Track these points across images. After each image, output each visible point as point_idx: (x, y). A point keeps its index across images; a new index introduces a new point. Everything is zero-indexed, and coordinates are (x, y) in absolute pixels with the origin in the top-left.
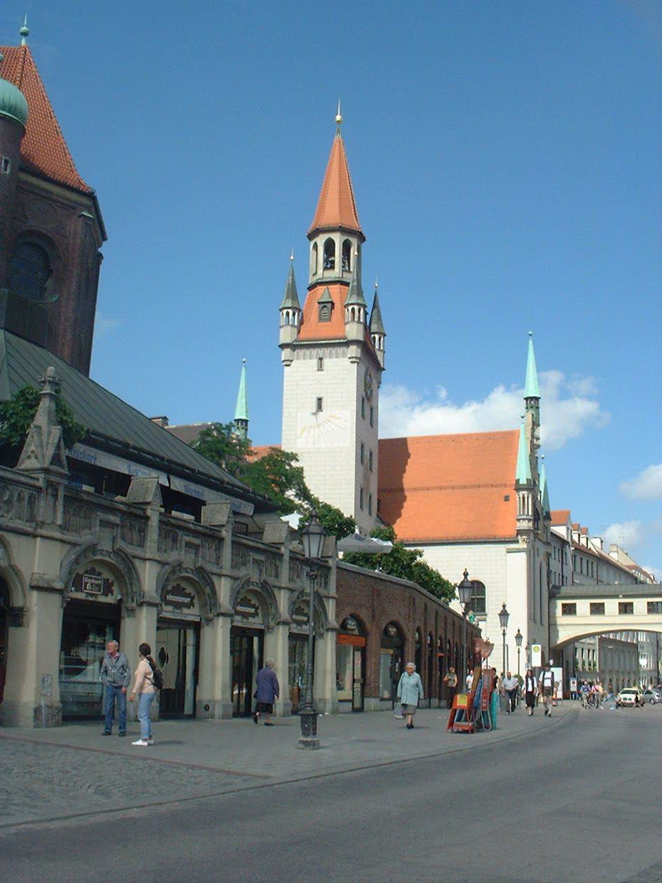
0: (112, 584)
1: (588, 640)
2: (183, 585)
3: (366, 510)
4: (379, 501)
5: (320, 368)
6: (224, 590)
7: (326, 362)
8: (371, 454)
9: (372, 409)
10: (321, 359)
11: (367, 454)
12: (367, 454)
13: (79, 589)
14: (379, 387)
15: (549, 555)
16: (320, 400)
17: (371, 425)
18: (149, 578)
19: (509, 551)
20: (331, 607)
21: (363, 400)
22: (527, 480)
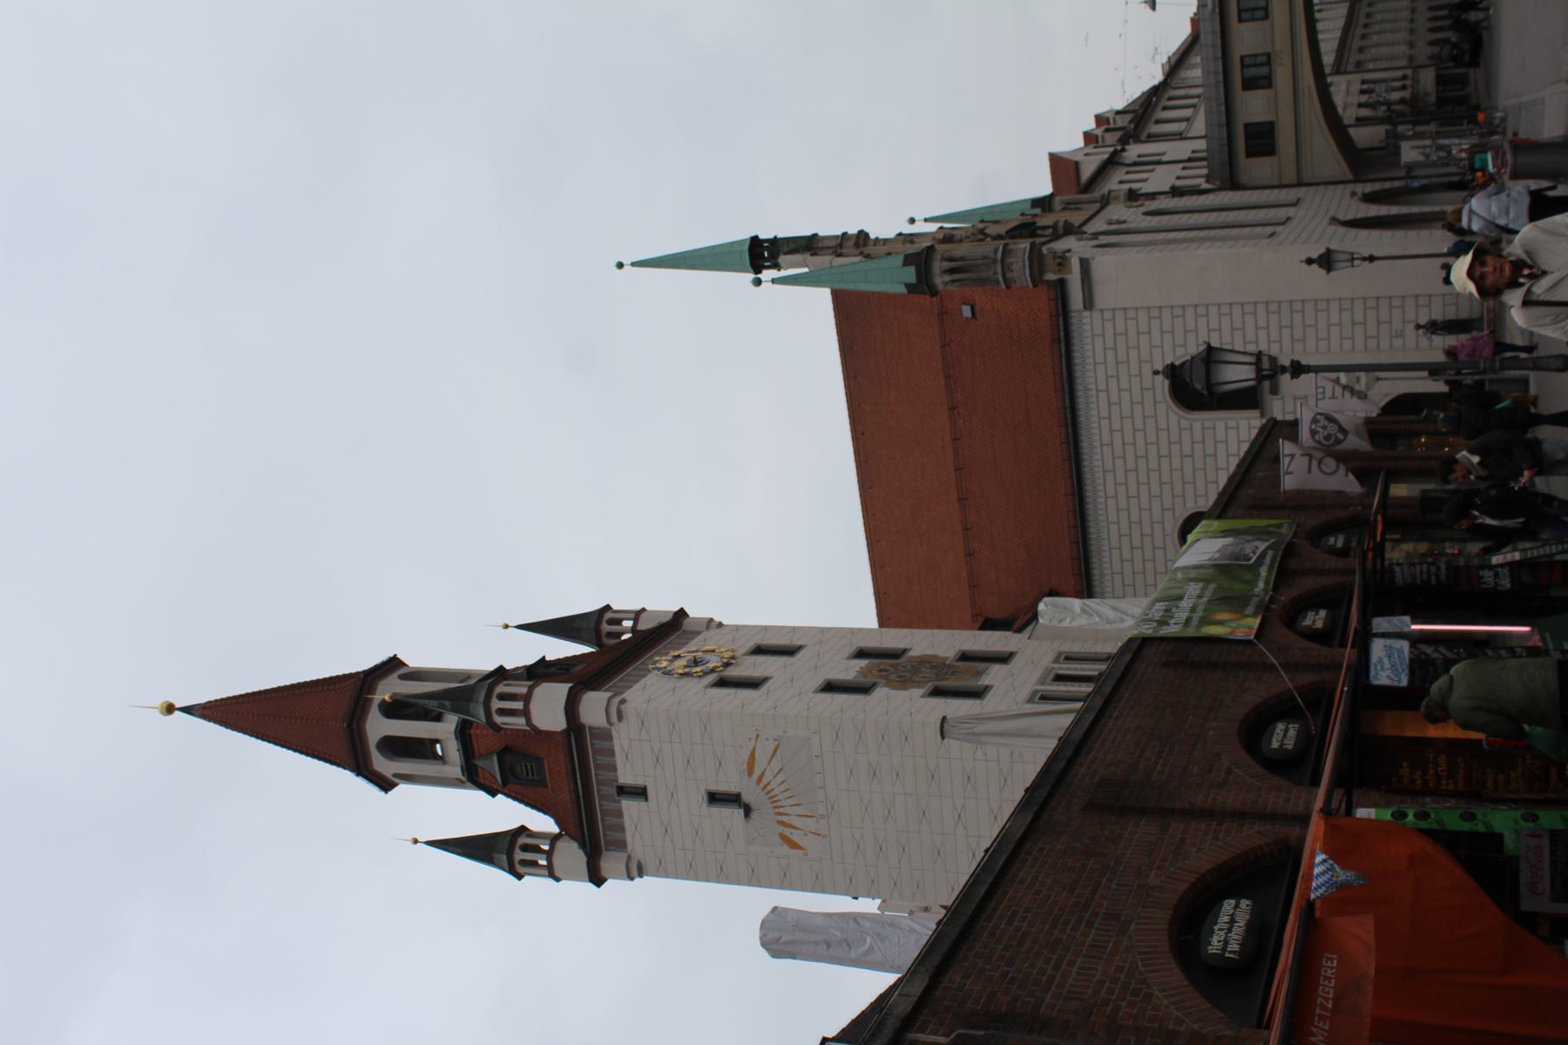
1: (1338, 99)
3: (994, 675)
4: (989, 624)
5: (640, 793)
7: (626, 777)
8: (861, 654)
9: (759, 650)
10: (623, 791)
11: (851, 671)
14: (720, 625)
15: (1133, 196)
16: (714, 798)
17: (789, 651)
19: (1089, 303)
21: (722, 683)
22: (905, 264)
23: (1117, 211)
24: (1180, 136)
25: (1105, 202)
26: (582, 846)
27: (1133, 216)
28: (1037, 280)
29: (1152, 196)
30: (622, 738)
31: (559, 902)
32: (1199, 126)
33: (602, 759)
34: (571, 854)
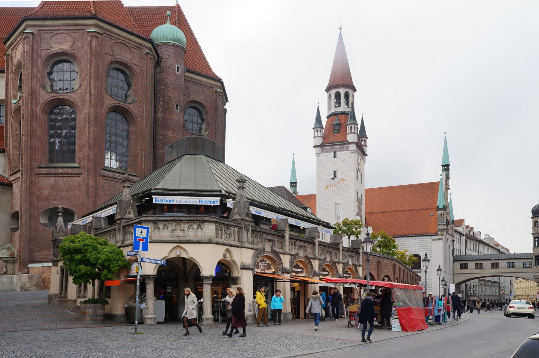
0: (271, 265)
2: (298, 264)
5: (335, 157)
6: (316, 264)
7: (338, 154)
10: (335, 152)
11: (359, 196)
12: (359, 196)
13: (258, 268)
15: (453, 241)
16: (335, 172)
18: (286, 260)
19: (433, 240)
20: (360, 270)
23: (450, 238)
24: (466, 248)
25: (452, 236)
26: (322, 144)
27: (449, 243)
28: (438, 231)
29: (453, 245)
30: (346, 153)
31: (309, 138)
32: (469, 252)
33: (342, 149)
34: (320, 141)
